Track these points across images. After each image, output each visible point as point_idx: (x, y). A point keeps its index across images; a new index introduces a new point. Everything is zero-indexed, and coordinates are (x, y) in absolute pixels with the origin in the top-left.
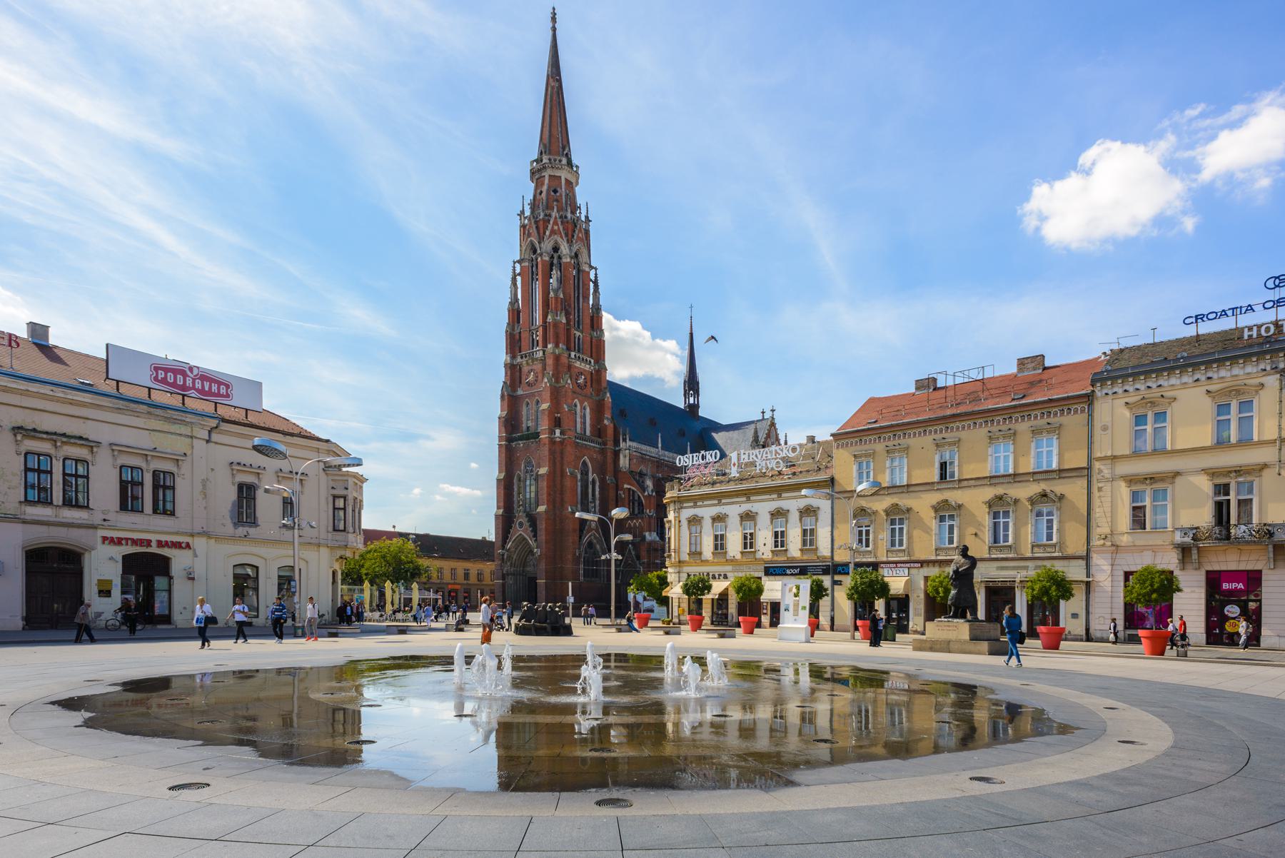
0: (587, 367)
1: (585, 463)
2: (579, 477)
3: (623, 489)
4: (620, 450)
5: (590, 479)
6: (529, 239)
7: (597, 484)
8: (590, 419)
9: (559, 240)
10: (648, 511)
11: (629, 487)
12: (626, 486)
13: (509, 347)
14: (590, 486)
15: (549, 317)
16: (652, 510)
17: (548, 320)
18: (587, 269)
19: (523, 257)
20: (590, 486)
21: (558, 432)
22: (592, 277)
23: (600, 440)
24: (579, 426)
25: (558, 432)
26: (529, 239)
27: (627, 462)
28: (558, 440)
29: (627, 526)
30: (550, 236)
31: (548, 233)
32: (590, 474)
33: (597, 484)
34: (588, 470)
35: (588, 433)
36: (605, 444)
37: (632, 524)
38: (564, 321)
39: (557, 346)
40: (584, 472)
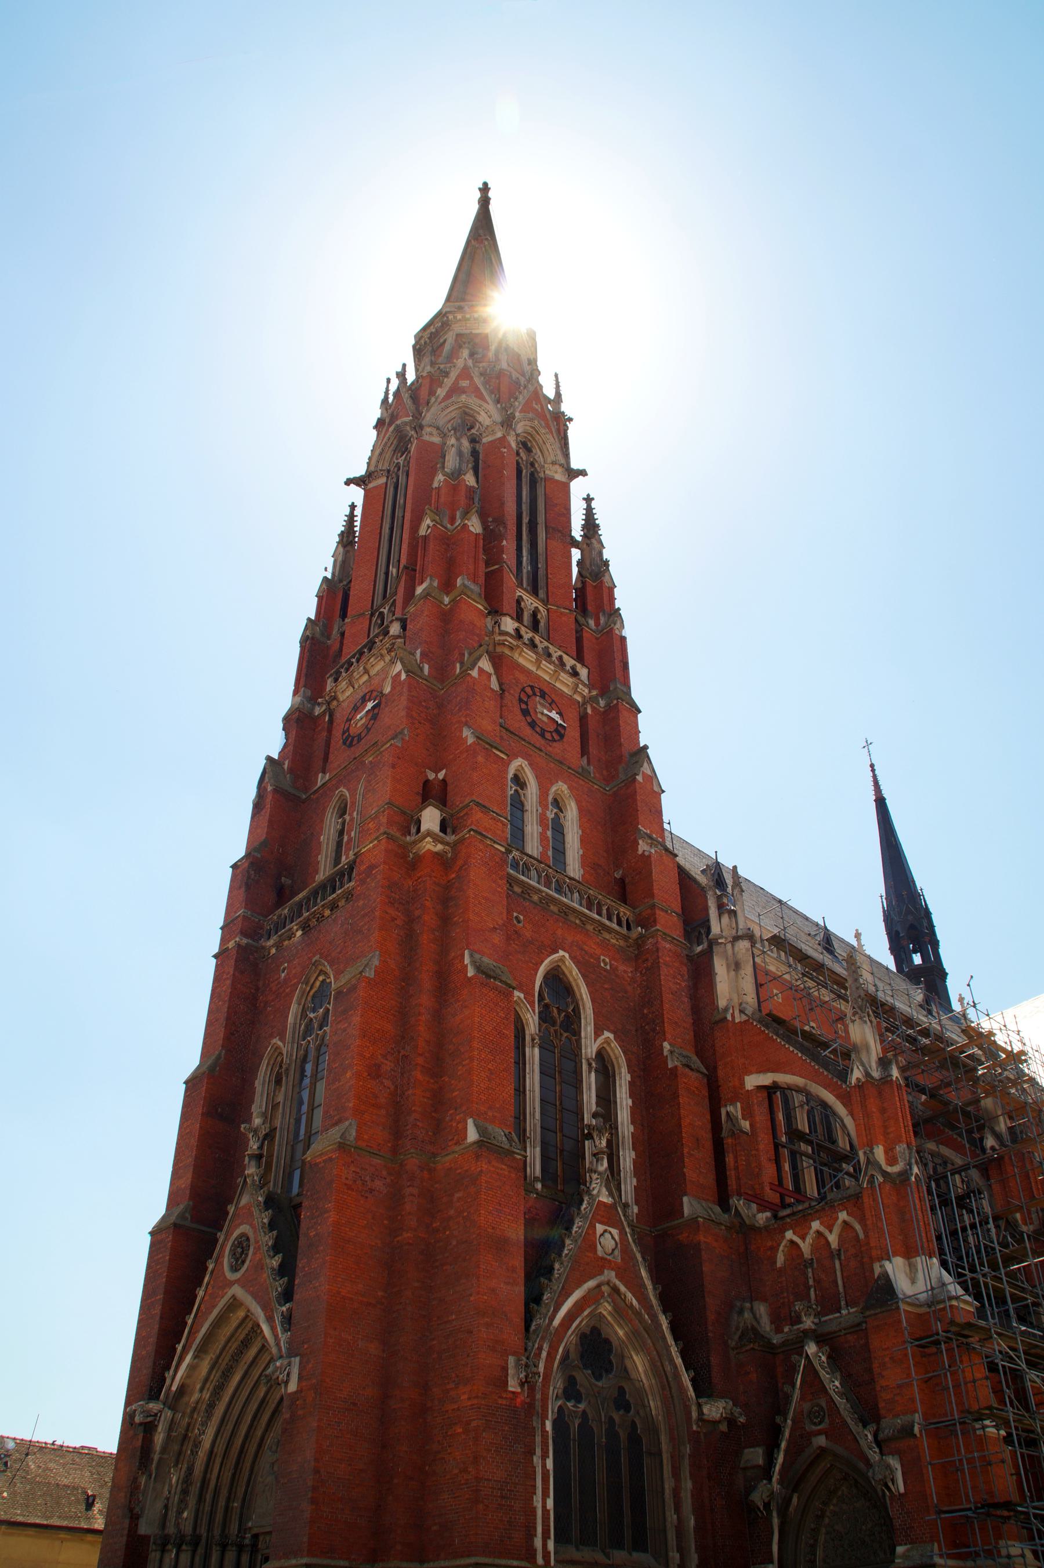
0: (564, 684)
1: (556, 980)
2: (532, 1022)
3: (739, 1094)
4: (712, 943)
5: (590, 1047)
6: (391, 429)
7: (623, 1080)
8: (584, 841)
9: (472, 401)
10: (879, 1153)
11: (766, 1079)
12: (752, 1081)
13: (305, 664)
14: (590, 1081)
15: (427, 522)
16: (901, 1148)
17: (422, 531)
18: (559, 476)
19: (372, 469)
20: (590, 1081)
21: (431, 818)
22: (577, 533)
23: (625, 912)
24: (532, 829)
25: (431, 818)
26: (391, 429)
27: (748, 985)
28: (429, 845)
29: (780, 1259)
30: (448, 396)
31: (441, 392)
32: (587, 1028)
33: (623, 1080)
34: (577, 1011)
35: (574, 868)
36: (647, 921)
37: (805, 1246)
38: (475, 526)
39: (447, 586)
40: (559, 1018)
